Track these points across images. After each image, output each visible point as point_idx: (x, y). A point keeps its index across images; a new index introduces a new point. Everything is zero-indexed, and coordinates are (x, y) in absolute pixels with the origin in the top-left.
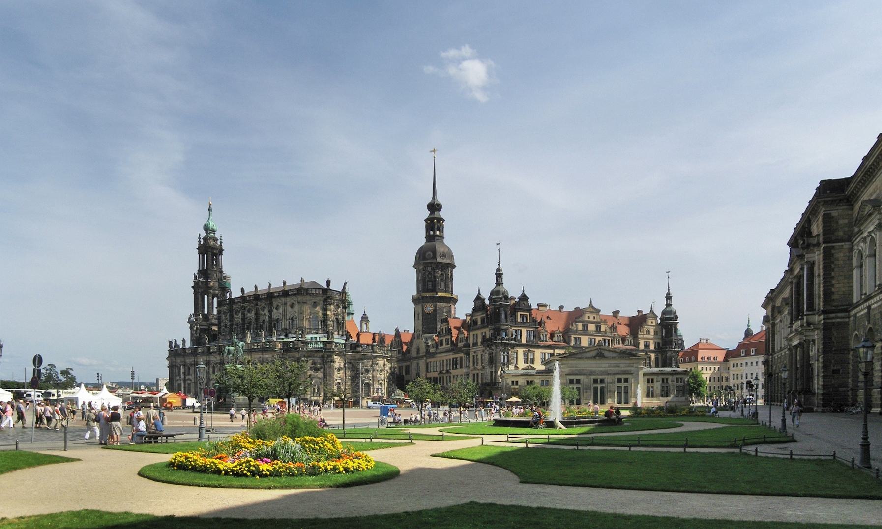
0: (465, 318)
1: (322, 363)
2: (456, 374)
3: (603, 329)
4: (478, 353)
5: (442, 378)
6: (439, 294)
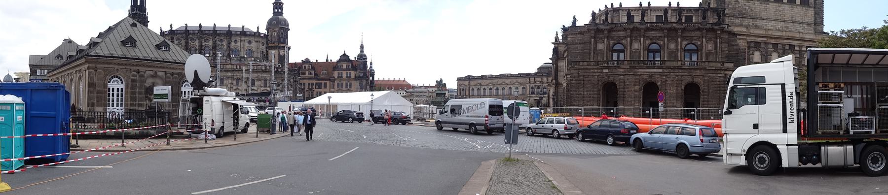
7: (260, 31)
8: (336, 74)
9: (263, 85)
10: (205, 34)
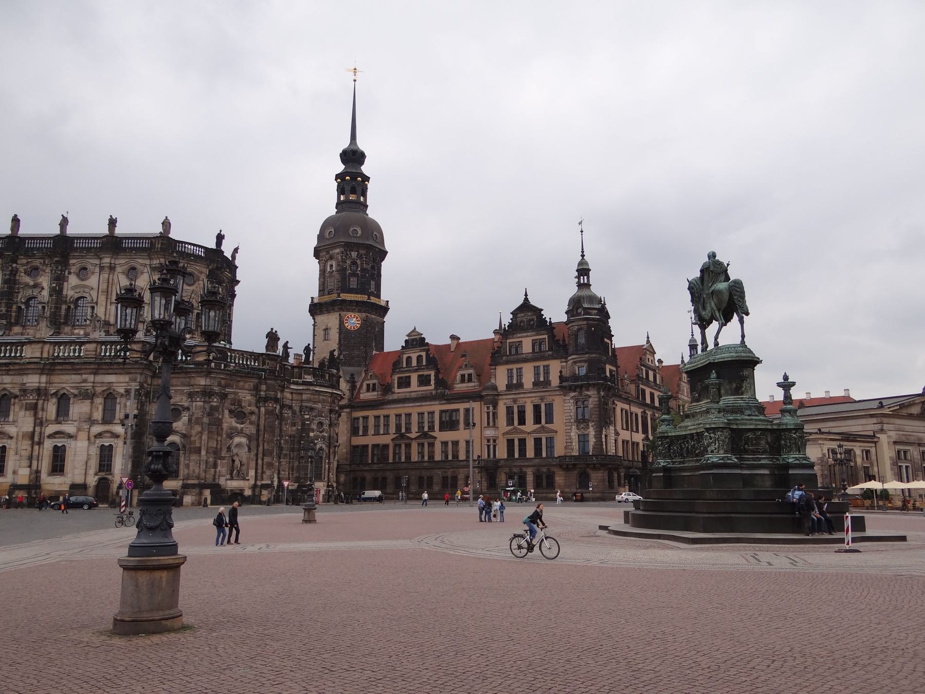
0: (448, 341)
1: (254, 401)
2: (455, 439)
3: (658, 382)
4: (526, 402)
5: (403, 446)
6: (373, 300)
7: (174, 235)
8: (500, 377)
9: (98, 415)
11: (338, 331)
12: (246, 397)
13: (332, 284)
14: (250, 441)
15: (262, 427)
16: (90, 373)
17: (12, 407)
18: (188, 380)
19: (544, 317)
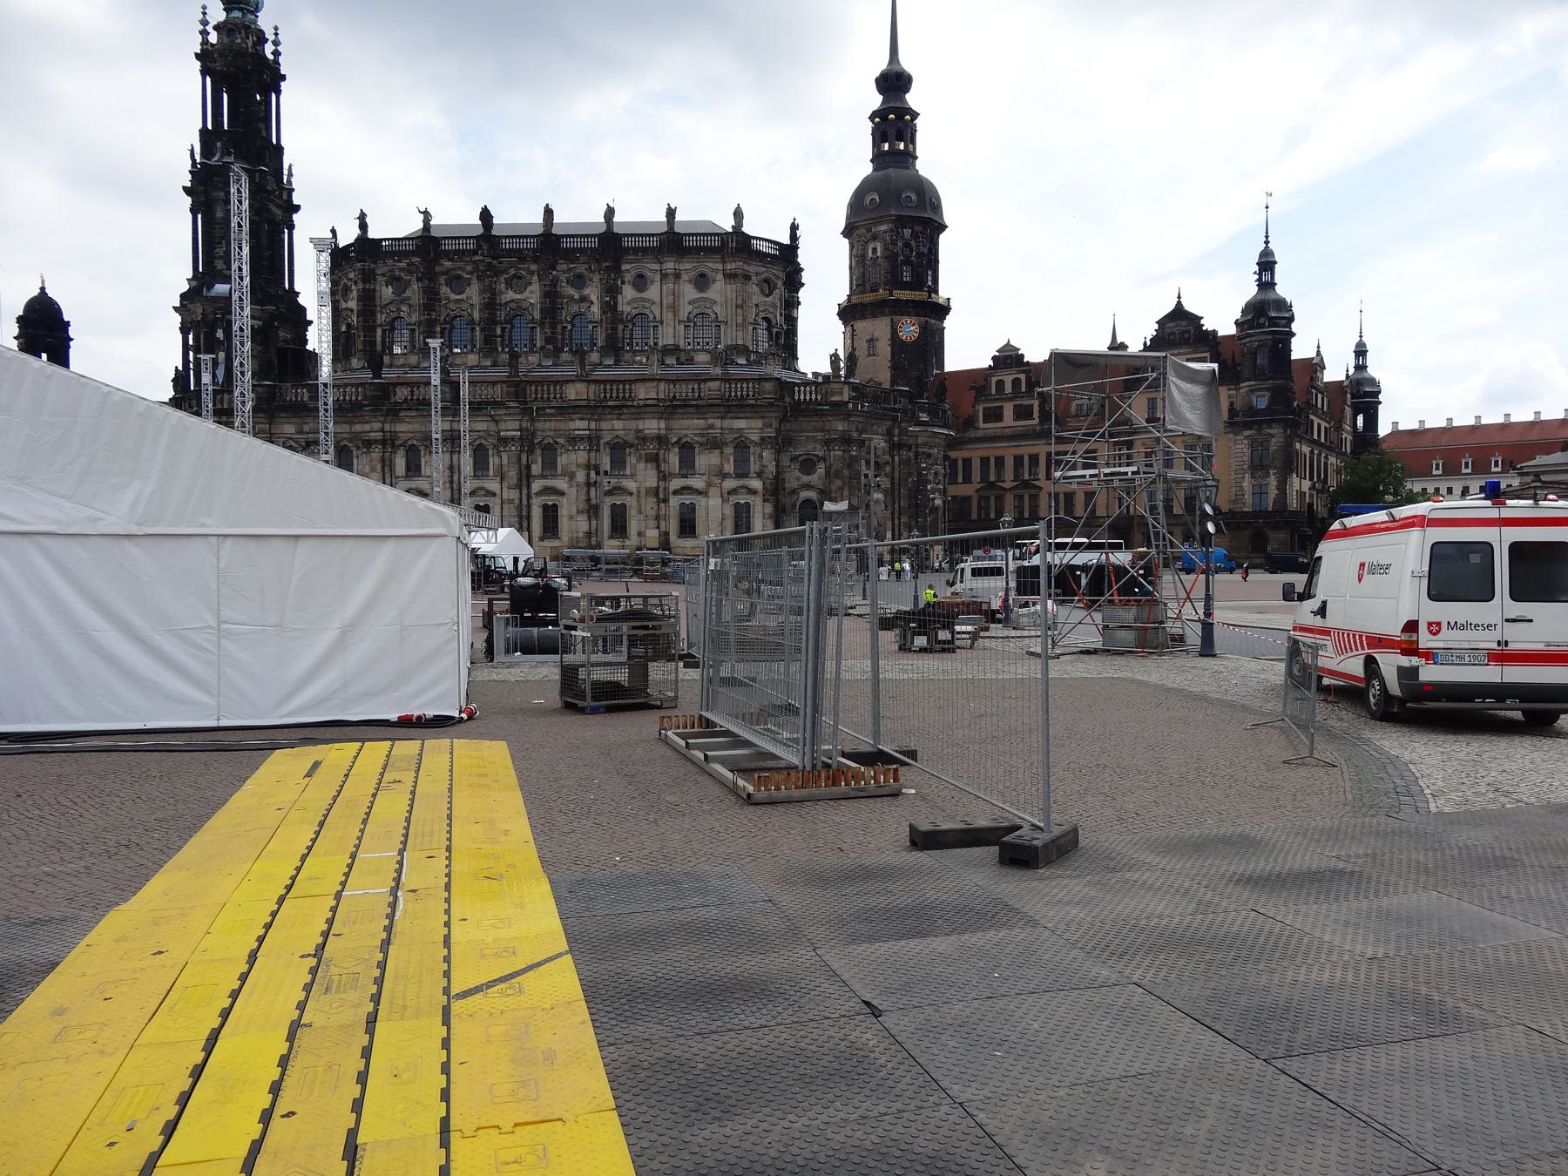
5: (993, 499)
9: (729, 467)
10: (510, 253)
11: (889, 342)
12: (879, 442)
13: (879, 274)
14: (885, 497)
15: (896, 480)
16: (717, 418)
17: (628, 458)
18: (821, 424)
19: (1204, 328)
